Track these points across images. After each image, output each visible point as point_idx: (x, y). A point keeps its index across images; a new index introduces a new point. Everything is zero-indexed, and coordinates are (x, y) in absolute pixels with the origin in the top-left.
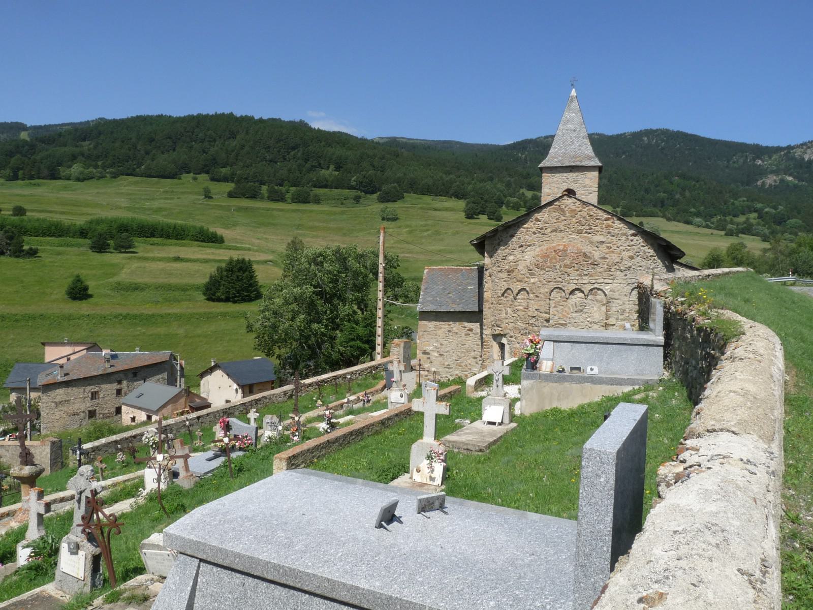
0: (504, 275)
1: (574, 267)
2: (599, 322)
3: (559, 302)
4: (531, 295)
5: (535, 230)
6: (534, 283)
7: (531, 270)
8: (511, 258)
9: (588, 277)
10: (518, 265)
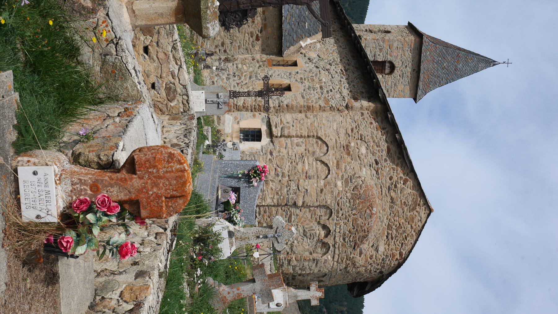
0: (343, 140)
1: (354, 228)
2: (292, 250)
3: (315, 214)
4: (322, 182)
5: (395, 178)
6: (336, 185)
7: (351, 180)
8: (363, 150)
9: (342, 241)
10: (356, 160)
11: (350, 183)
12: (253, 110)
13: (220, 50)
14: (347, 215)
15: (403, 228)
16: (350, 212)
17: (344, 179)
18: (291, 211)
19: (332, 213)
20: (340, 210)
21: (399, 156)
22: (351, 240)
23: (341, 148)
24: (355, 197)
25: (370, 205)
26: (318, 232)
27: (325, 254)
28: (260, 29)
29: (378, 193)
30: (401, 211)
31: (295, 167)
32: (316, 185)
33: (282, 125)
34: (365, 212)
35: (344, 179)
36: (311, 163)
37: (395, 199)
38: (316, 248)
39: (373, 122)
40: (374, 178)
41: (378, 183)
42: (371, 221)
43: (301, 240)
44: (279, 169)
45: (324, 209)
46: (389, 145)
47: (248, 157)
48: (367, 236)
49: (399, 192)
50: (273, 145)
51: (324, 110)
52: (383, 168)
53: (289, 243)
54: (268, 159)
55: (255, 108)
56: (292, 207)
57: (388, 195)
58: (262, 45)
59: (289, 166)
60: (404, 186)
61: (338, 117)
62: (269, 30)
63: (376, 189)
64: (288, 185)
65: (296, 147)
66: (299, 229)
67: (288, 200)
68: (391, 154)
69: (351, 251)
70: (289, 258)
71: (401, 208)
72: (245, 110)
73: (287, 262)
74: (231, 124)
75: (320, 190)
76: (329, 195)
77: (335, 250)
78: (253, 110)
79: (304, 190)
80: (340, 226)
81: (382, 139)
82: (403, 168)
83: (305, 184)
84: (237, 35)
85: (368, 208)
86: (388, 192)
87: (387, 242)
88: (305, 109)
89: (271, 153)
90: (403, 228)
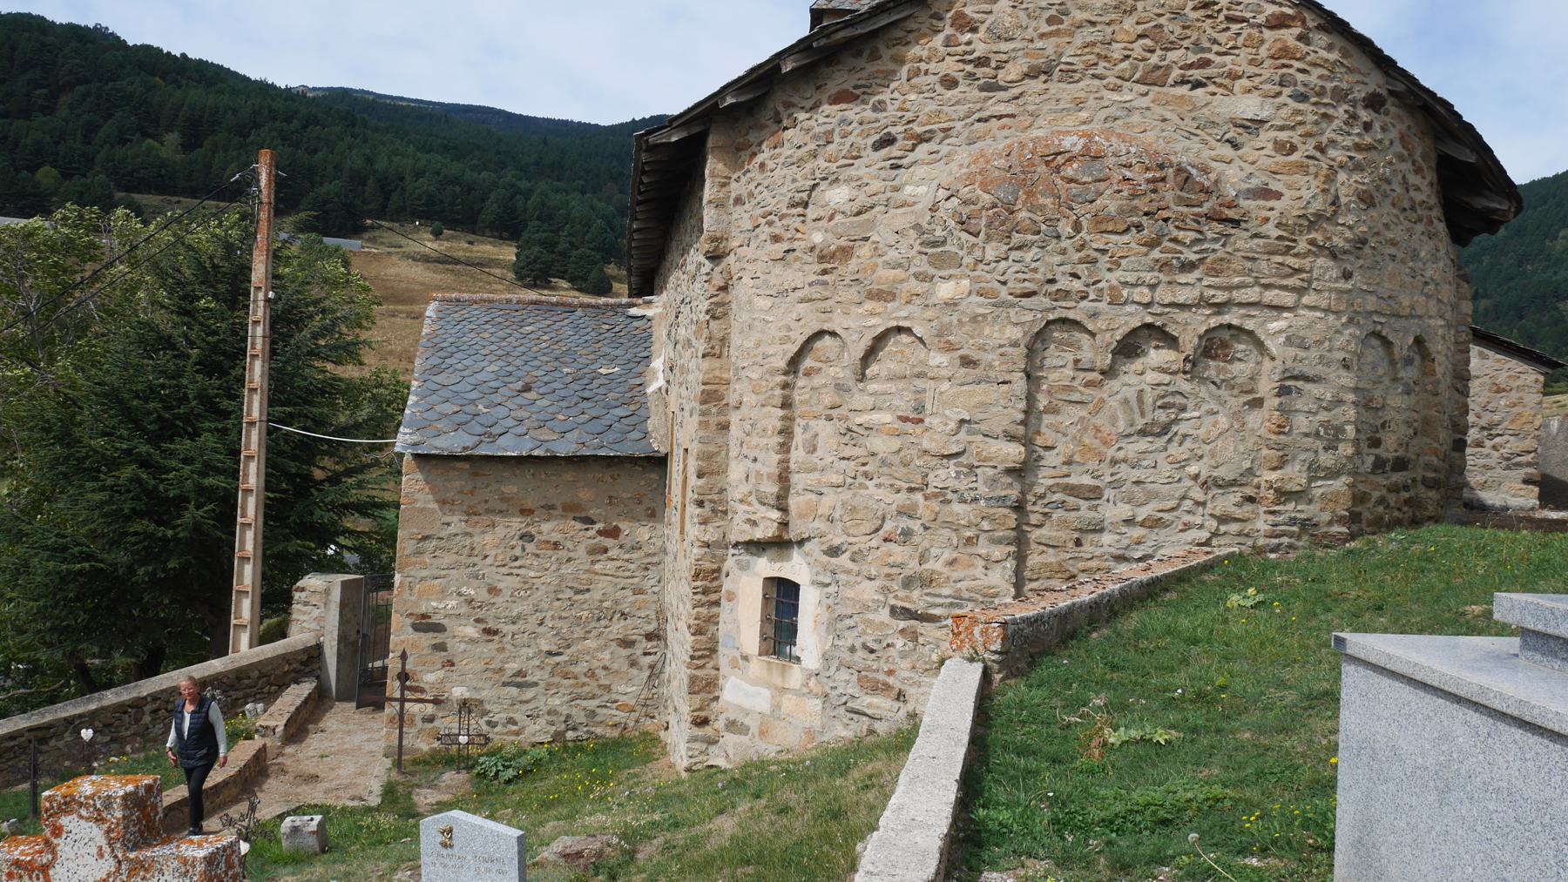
0: (801, 274)
1: (1139, 227)
2: (1234, 483)
3: (1069, 389)
4: (938, 359)
5: (951, 66)
6: (952, 304)
7: (935, 244)
8: (837, 196)
9: (1197, 274)
10: (872, 224)
11: (947, 248)
12: (713, 597)
13: (645, 654)
14: (1076, 256)
15: (1162, 21)
16: (1065, 244)
17: (931, 271)
18: (1050, 488)
19: (1064, 321)
20: (1053, 288)
21: (866, 53)
22: (1193, 235)
23: (825, 283)
24: (1003, 224)
25: (1047, 163)
26: (1151, 377)
27: (1260, 345)
28: (579, 525)
29: (1006, 132)
30: (1088, 35)
31: (883, 462)
32: (945, 386)
33: (753, 499)
34: (1071, 181)
35: (931, 271)
36: (870, 401)
37: (1035, 62)
38: (1230, 384)
39: (760, 158)
40: (945, 149)
41: (966, 134)
42: (1115, 155)
43: (1188, 444)
44: (888, 526)
45: (1046, 353)
46: (825, 97)
47: (840, 643)
48: (1180, 170)
49: (1004, 46)
50: (809, 539)
51: (723, 340)
52: (909, 115)
53: (1198, 494)
54: (850, 565)
55: (705, 592)
56: (1032, 485)
57: (1016, 91)
58: (635, 519)
59: (879, 486)
60: (983, 29)
61: (742, 291)
62: (584, 495)
63: (989, 141)
64: (942, 496)
65: (819, 453)
66: (1131, 455)
67: (999, 499)
68: (856, 87)
69: (1247, 235)
70: (1271, 494)
71: (1072, 34)
72: (712, 628)
73: (1291, 506)
74: (745, 686)
75: (963, 371)
76: (987, 331)
77: (1241, 305)
78: (713, 597)
79: (962, 435)
80: (1126, 284)
81: (806, 124)
82: (911, 37)
83: (938, 432)
84: (597, 595)
85: (1058, 170)
86: (1006, 89)
87: (1220, 85)
88: (714, 410)
89: (834, 551)
90: (1162, 21)
